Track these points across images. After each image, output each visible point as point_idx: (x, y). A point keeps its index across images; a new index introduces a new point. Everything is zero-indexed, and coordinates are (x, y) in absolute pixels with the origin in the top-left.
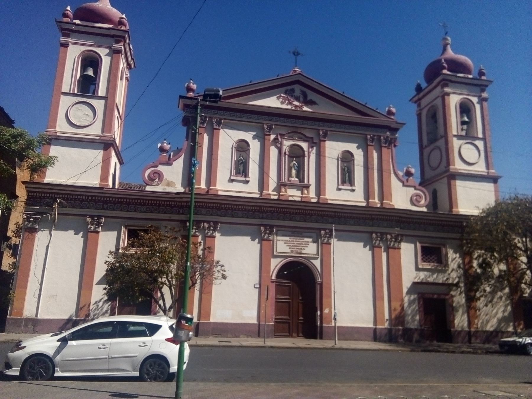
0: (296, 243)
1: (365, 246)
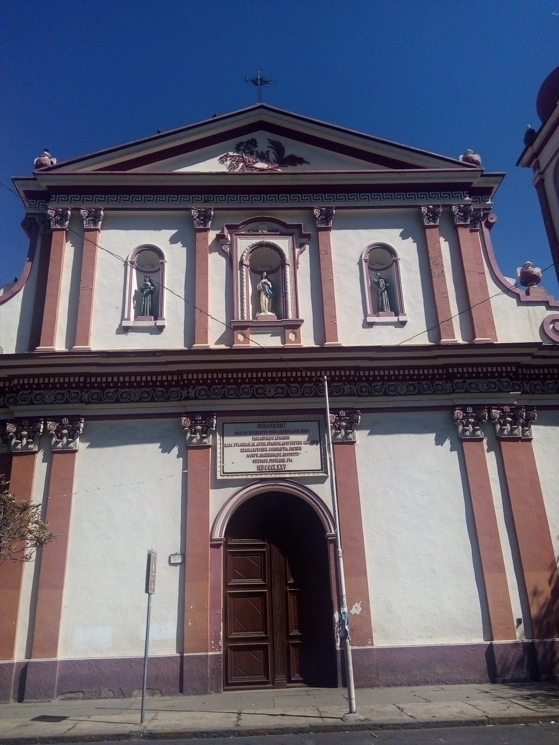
0: (268, 447)
1: (439, 441)
